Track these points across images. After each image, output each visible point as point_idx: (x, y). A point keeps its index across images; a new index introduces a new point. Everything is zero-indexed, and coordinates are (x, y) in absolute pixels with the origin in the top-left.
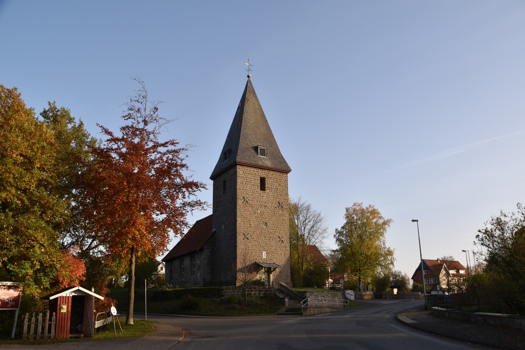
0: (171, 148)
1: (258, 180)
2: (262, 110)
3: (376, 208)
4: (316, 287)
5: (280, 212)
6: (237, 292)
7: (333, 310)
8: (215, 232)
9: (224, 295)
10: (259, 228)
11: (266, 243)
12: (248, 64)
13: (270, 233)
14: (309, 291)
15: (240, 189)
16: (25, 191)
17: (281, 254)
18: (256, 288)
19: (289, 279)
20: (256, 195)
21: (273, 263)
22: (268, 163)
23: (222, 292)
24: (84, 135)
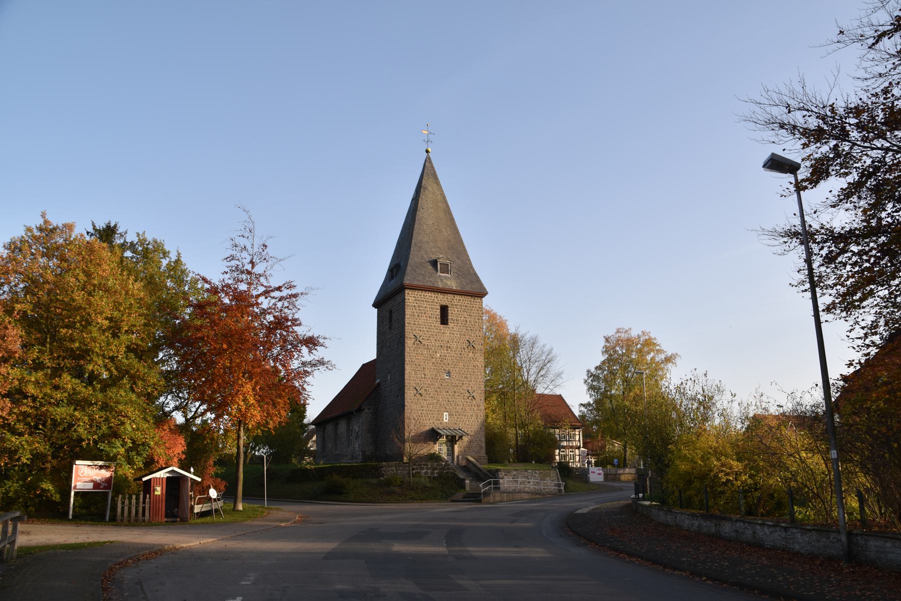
0: (285, 292)
1: (437, 309)
2: (446, 202)
3: (652, 335)
4: (534, 462)
5: (471, 354)
6: (402, 470)
7: (534, 497)
8: (379, 384)
9: (383, 474)
10: (437, 379)
11: (448, 401)
12: (427, 133)
13: (454, 386)
14: (504, 470)
15: (410, 324)
16: (112, 359)
17: (472, 416)
18: (427, 465)
19: (483, 451)
20: (434, 332)
21: (459, 429)
22: (453, 284)
23: (381, 471)
24: (183, 272)
